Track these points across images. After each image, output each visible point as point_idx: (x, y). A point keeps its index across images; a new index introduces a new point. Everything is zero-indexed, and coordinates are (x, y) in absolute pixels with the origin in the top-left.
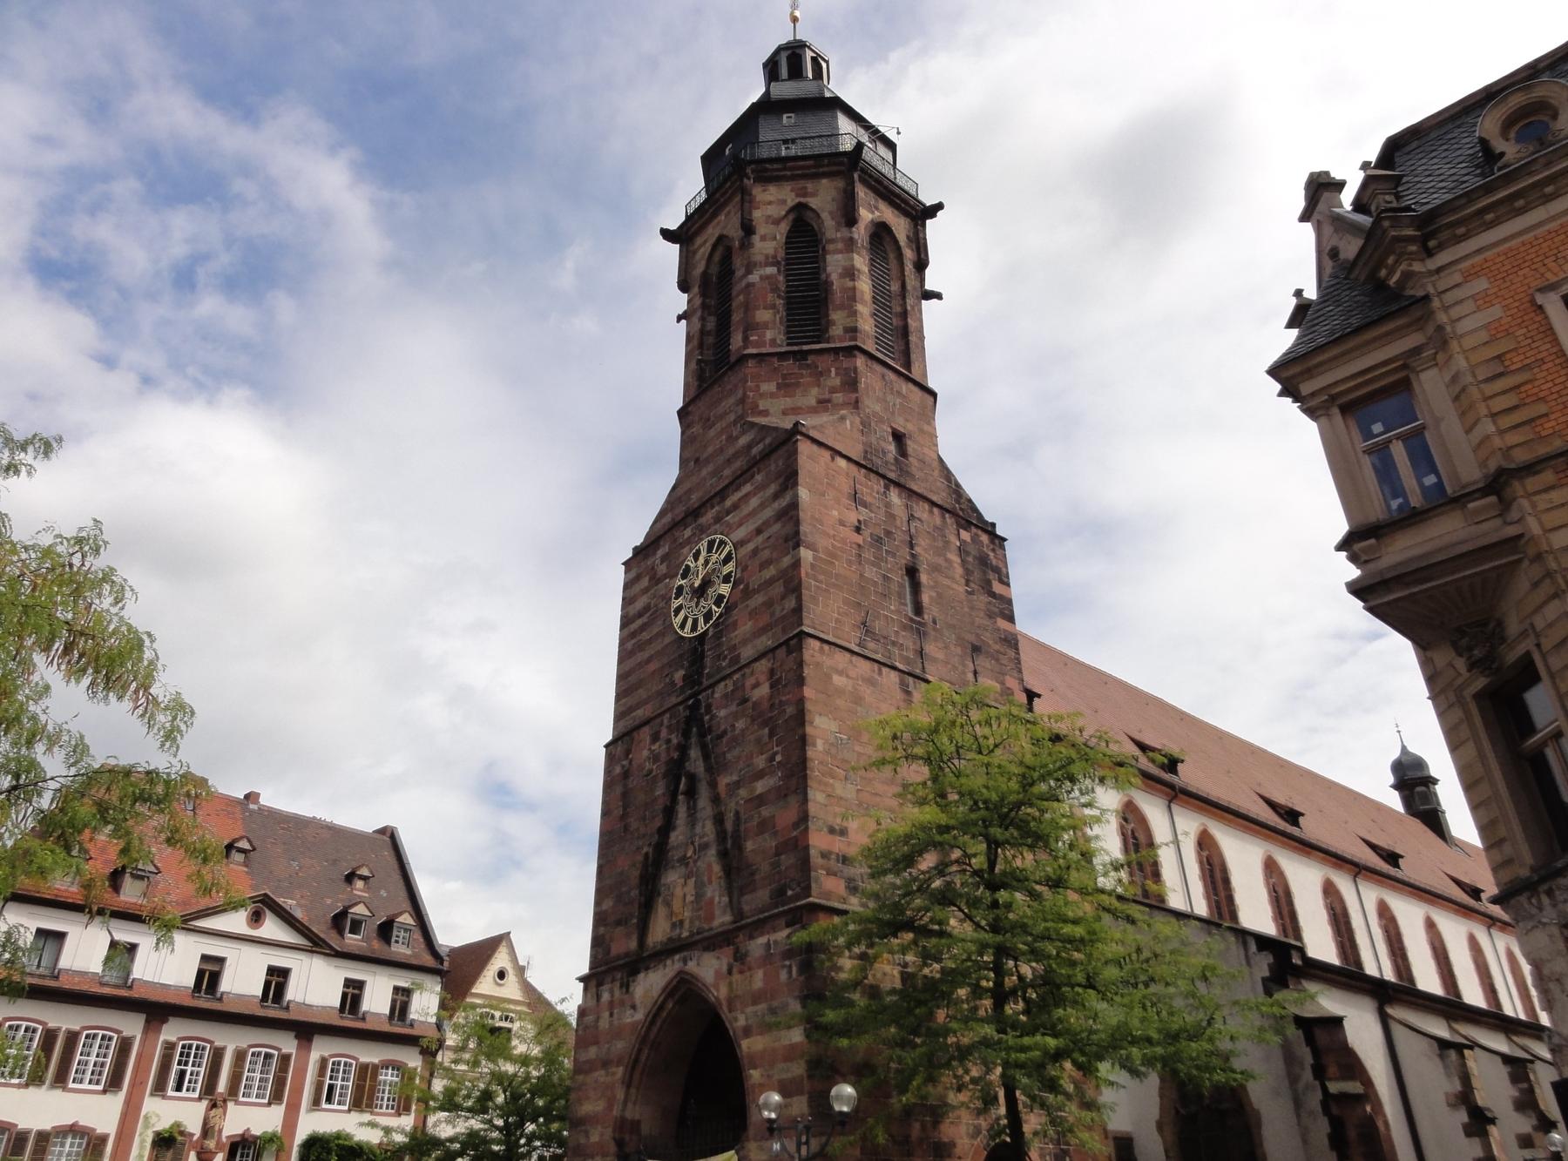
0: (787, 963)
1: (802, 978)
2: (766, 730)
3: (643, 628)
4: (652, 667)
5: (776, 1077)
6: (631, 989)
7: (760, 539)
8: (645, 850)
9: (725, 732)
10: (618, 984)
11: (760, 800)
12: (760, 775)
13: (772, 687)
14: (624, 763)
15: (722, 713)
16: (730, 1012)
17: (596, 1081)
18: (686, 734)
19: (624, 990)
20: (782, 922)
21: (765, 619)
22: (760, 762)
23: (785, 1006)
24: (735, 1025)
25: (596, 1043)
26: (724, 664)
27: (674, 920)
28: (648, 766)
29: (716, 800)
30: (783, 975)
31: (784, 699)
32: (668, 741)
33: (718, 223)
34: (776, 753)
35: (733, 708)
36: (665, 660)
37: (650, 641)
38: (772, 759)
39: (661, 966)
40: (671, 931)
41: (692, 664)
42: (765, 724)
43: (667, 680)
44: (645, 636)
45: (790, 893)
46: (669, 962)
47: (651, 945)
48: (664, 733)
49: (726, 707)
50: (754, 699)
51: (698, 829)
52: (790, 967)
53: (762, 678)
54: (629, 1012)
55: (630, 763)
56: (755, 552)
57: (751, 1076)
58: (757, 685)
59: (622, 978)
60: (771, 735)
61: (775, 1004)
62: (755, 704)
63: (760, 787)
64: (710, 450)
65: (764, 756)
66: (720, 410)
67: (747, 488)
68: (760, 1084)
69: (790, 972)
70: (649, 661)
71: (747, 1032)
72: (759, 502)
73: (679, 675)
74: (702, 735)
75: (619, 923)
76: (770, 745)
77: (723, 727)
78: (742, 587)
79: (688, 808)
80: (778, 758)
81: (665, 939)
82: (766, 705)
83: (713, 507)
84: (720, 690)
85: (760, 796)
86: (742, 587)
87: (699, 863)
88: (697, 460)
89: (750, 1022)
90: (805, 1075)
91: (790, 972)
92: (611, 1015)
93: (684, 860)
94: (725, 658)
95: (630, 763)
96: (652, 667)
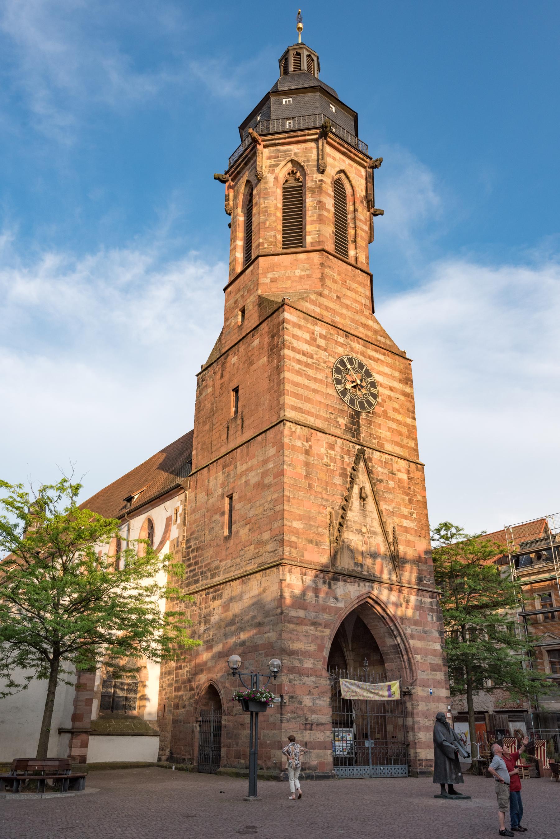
0: (431, 613)
1: (438, 623)
2: (407, 498)
3: (307, 365)
4: (318, 398)
5: (429, 661)
6: (333, 587)
7: (392, 394)
8: (329, 509)
9: (381, 481)
10: (321, 580)
11: (406, 530)
12: (405, 517)
13: (409, 479)
14: (305, 443)
15: (380, 469)
16: (402, 624)
17: (307, 632)
18: (357, 462)
19: (327, 586)
20: (427, 594)
21: (397, 439)
22: (405, 511)
23: (431, 632)
24: (405, 631)
25: (305, 609)
26: (374, 441)
27: (356, 561)
28: (325, 460)
29: (380, 513)
30: (429, 618)
31: (416, 489)
32: (342, 457)
33: (344, 161)
34: (413, 513)
35: (386, 471)
36: (329, 403)
37: (316, 380)
38: (412, 514)
39: (356, 584)
40: (355, 566)
41: (353, 423)
42: (408, 494)
43: (333, 417)
44: (310, 372)
45: (425, 582)
46: (362, 584)
47: (340, 568)
48: (338, 449)
49: (382, 468)
50: (400, 477)
51: (368, 520)
52: (432, 616)
53: (403, 470)
54: (331, 600)
55: (310, 447)
56: (390, 397)
57: (416, 657)
58: (399, 471)
59: (324, 578)
60: (410, 501)
61: (426, 629)
62: (400, 480)
63: (406, 523)
64: (348, 302)
65: (407, 510)
66: (355, 286)
67: (381, 357)
68: (421, 663)
69: (432, 618)
70: (315, 391)
71: (412, 637)
72: (389, 373)
73: (342, 421)
74: (369, 472)
75: (311, 542)
76: (410, 507)
77: (380, 477)
78: (383, 409)
79: (361, 506)
80: (415, 516)
81: (350, 569)
82: (406, 485)
83: (359, 343)
84: (376, 455)
85: (406, 527)
86: (383, 409)
87: (371, 540)
88: (338, 297)
89: (414, 633)
90: (442, 664)
91: (432, 618)
92: (317, 596)
93: (360, 532)
94: (375, 439)
95: (310, 447)
96: (318, 398)
